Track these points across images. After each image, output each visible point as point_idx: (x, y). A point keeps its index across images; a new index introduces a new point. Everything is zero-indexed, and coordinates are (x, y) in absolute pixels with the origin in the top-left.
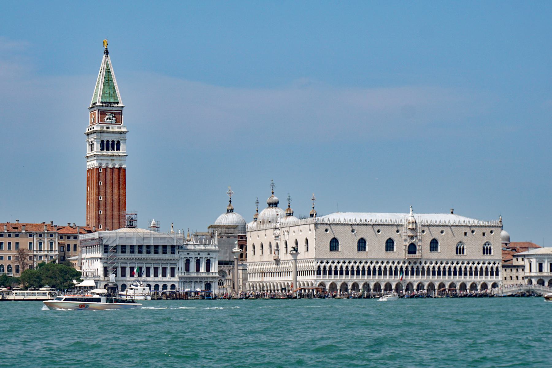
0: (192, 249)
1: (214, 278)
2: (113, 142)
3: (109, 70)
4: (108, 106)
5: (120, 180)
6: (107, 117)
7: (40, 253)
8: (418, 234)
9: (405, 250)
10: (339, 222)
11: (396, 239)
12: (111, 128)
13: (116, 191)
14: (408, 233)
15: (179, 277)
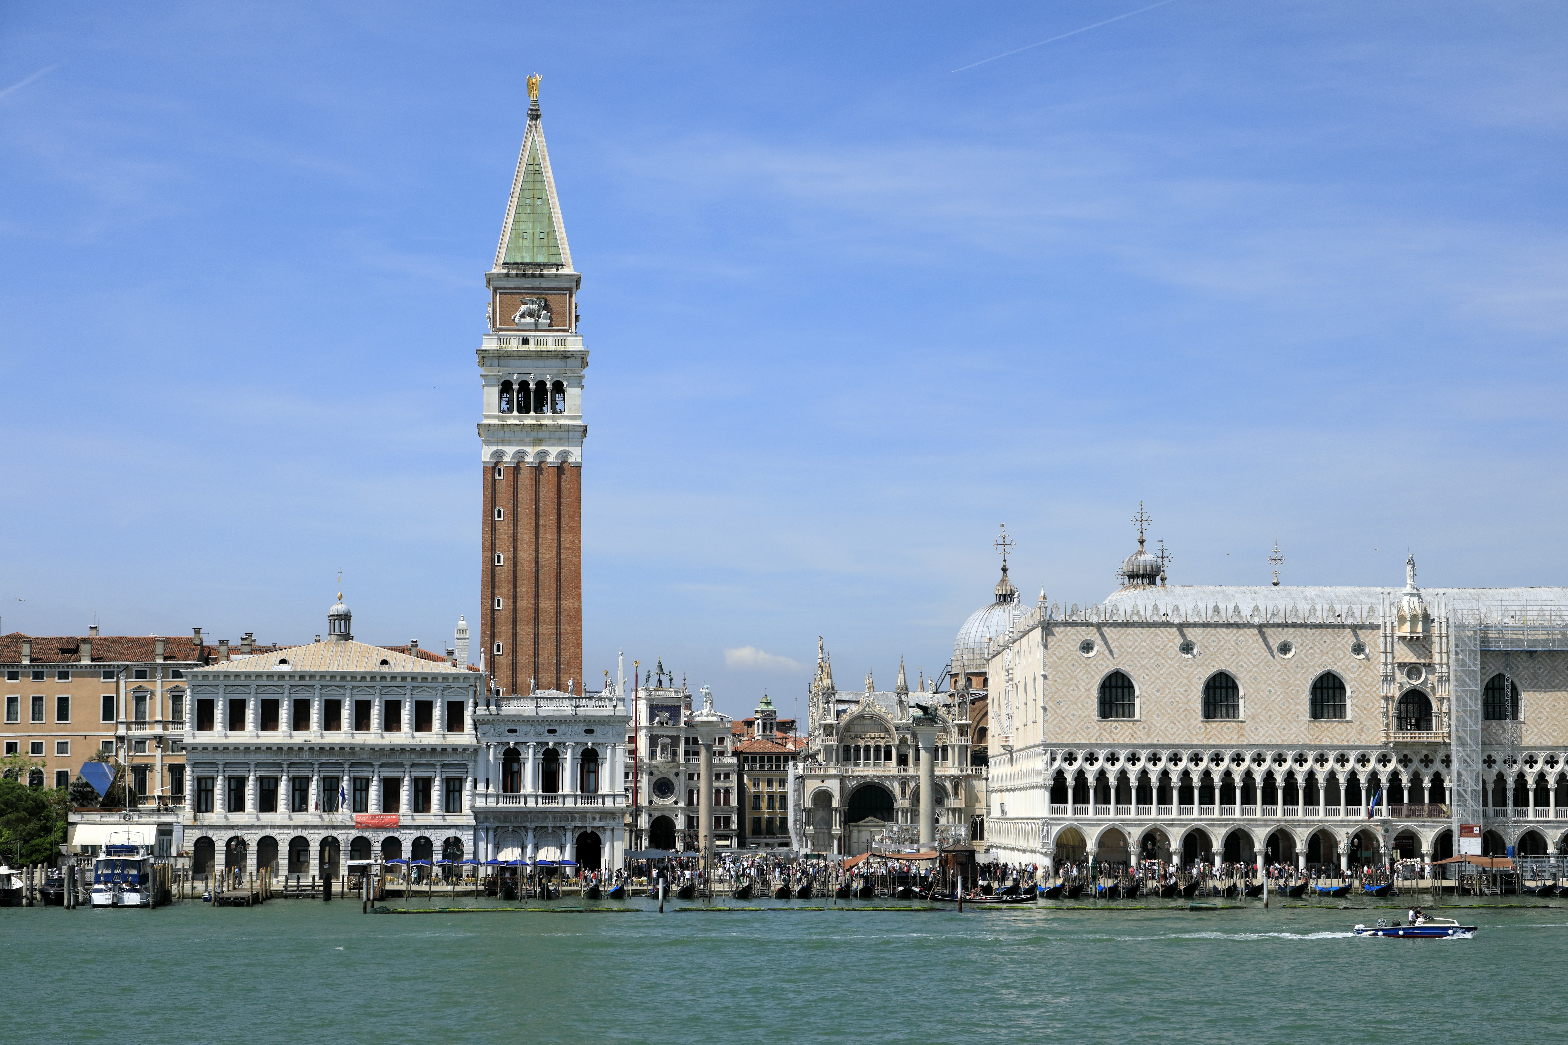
0: (527, 713)
1: (611, 814)
2: (541, 384)
3: (537, 168)
4: (524, 275)
5: (564, 501)
6: (523, 308)
7: (136, 732)
8: (1436, 658)
9: (1386, 714)
10: (1135, 618)
11: (1353, 676)
12: (532, 341)
13: (548, 536)
14: (1397, 654)
15: (477, 814)
